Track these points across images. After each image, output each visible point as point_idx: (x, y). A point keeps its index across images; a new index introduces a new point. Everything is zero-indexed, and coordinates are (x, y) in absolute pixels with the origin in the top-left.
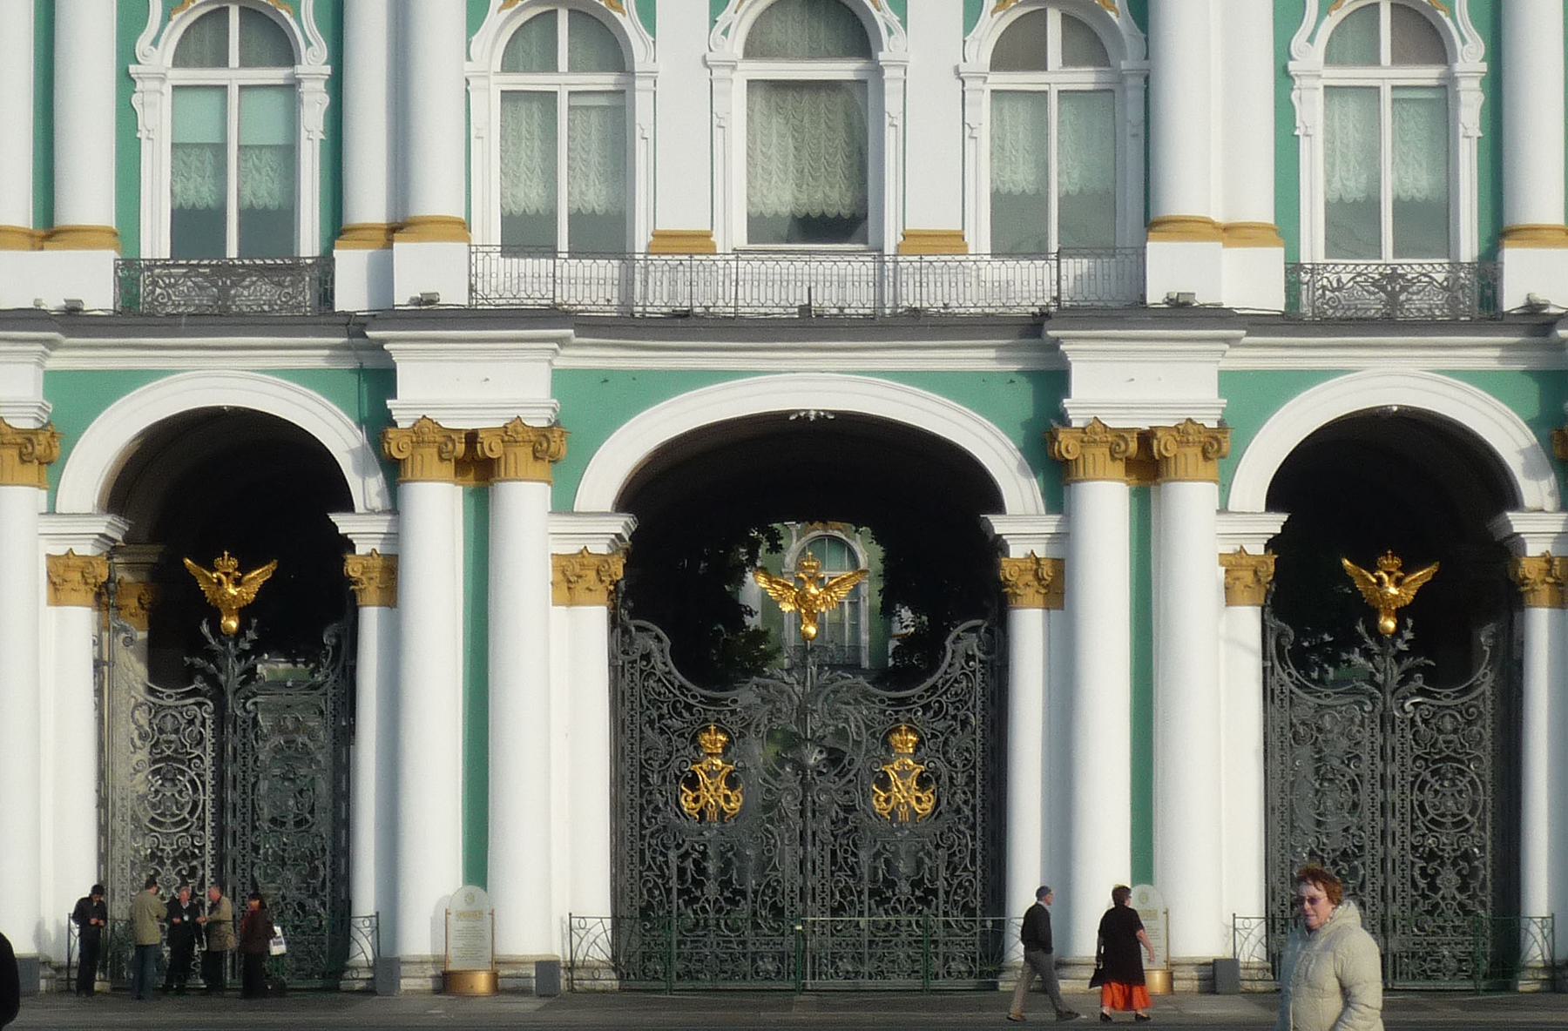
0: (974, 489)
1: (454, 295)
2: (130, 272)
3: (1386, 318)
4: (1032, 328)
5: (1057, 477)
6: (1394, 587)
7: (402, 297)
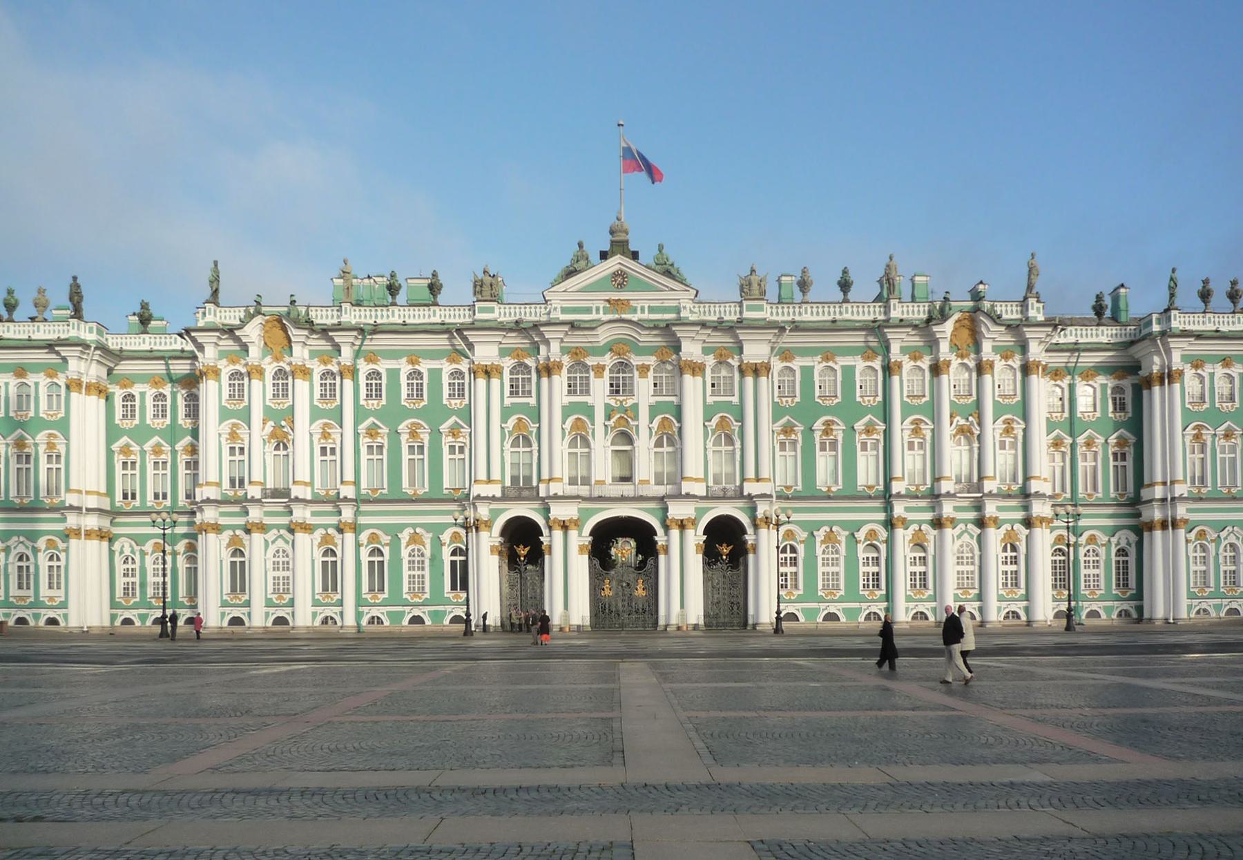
0: (651, 531)
1: (560, 493)
2: (503, 488)
3: (724, 497)
4: (662, 499)
5: (666, 528)
6: (725, 550)
7: (551, 494)
